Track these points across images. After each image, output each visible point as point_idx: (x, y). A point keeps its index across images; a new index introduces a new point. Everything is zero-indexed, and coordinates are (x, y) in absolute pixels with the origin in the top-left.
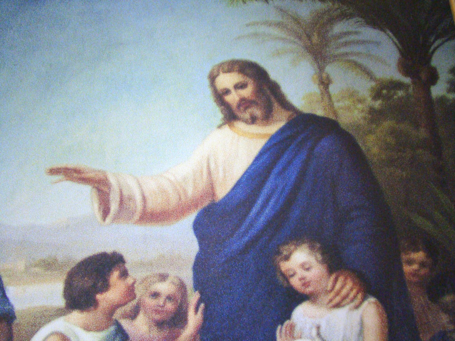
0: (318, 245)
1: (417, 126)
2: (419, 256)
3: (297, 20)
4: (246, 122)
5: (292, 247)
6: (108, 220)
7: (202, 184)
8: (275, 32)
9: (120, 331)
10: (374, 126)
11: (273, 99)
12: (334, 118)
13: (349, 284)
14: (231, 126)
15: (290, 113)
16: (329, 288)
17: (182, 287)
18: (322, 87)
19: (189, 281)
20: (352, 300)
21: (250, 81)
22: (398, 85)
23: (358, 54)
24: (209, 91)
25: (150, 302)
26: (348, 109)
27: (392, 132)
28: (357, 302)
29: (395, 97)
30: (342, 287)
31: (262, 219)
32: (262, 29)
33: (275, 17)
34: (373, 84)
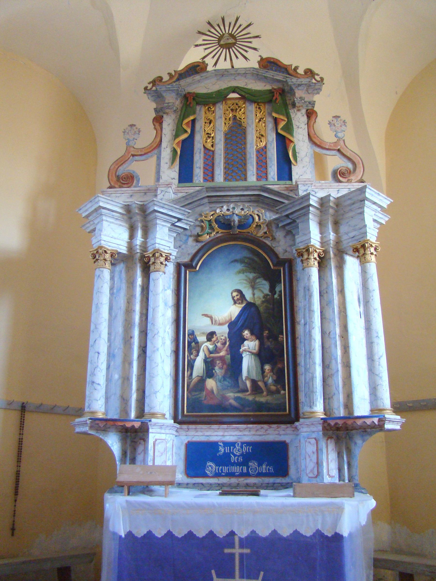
1: (270, 305)
2: (267, 332)
7: (230, 317)
8: (245, 282)
9: (216, 346)
14: (235, 305)
17: (226, 338)
19: (227, 337)
23: (261, 287)
24: (231, 297)
27: (266, 306)
32: (242, 281)
33: (246, 278)
34: (263, 295)
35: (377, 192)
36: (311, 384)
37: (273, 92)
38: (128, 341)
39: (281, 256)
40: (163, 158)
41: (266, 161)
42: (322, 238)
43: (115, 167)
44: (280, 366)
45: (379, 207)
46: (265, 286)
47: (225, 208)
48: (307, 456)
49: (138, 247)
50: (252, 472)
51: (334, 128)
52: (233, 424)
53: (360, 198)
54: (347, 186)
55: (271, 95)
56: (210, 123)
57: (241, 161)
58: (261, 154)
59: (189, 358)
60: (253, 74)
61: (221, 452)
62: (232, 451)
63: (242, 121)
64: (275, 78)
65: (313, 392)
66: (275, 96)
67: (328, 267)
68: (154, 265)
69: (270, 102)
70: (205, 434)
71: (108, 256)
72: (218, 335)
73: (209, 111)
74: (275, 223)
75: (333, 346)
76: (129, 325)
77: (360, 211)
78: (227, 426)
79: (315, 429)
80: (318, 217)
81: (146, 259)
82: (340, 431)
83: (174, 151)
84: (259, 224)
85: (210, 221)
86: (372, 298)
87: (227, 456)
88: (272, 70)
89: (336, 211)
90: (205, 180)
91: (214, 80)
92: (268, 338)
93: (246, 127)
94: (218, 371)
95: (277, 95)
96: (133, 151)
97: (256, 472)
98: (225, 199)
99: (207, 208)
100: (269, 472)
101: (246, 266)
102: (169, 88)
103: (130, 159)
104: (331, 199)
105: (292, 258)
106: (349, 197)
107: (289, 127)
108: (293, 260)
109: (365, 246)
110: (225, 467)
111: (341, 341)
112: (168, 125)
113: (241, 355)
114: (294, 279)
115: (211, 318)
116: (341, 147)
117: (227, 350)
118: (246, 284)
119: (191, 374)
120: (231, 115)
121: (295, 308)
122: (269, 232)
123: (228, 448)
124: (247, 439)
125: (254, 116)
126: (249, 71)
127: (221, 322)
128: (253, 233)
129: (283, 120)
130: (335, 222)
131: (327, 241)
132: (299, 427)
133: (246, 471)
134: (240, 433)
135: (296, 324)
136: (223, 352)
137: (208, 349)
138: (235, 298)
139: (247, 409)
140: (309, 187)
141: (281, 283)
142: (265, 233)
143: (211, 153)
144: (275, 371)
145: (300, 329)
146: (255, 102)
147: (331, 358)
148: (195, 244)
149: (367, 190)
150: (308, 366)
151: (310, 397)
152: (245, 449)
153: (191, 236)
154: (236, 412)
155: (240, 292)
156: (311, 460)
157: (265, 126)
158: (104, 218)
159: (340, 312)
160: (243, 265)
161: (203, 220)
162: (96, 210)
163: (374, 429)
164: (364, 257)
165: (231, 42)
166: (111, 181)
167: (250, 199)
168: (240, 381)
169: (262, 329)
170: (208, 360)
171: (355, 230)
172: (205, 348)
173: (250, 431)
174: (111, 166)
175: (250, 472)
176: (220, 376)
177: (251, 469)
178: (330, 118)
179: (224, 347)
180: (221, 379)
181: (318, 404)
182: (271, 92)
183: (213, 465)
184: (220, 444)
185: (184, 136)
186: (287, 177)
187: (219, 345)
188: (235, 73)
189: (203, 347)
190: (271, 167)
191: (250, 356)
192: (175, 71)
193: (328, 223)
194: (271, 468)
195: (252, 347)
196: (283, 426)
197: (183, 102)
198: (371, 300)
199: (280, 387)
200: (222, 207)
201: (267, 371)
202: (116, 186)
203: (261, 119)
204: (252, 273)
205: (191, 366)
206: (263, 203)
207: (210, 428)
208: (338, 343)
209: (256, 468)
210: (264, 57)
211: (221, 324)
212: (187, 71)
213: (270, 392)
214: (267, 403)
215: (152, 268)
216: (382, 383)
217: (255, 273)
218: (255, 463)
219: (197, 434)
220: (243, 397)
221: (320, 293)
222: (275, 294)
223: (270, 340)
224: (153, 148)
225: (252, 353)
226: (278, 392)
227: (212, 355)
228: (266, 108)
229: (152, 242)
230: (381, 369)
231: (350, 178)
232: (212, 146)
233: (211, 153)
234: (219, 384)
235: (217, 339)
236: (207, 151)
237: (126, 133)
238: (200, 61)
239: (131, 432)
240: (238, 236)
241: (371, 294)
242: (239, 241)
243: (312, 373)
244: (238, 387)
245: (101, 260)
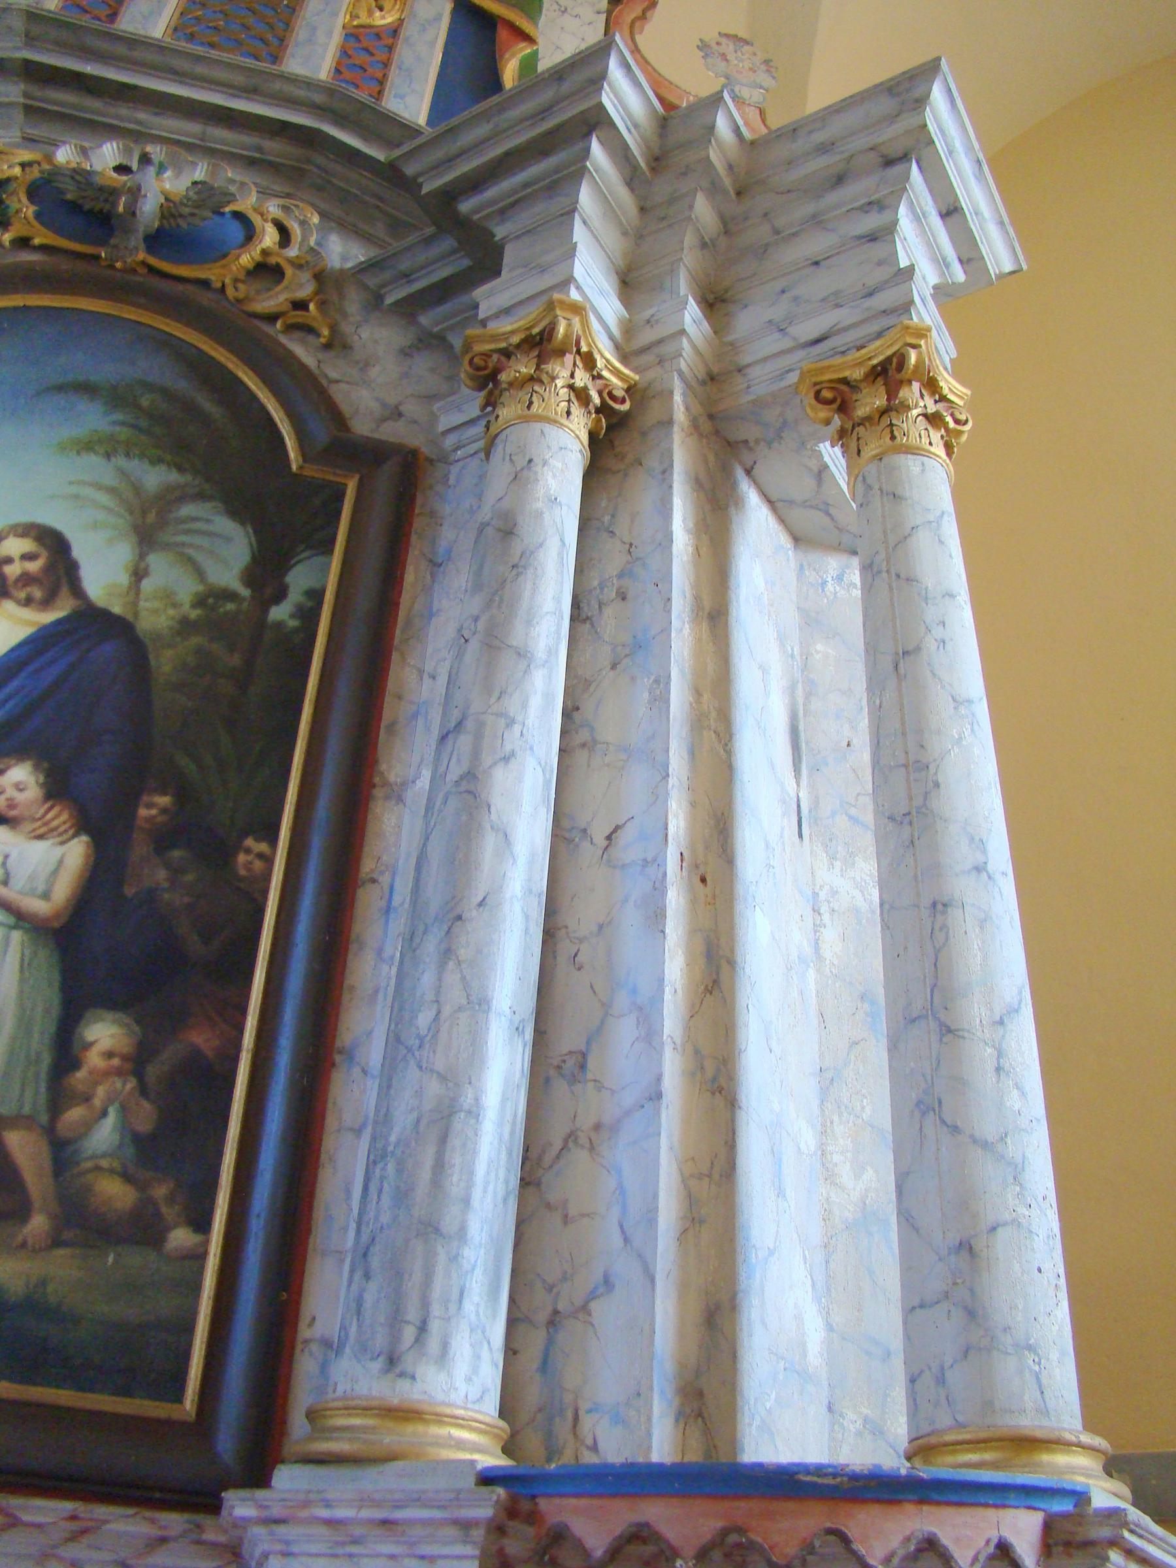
0: (46, 765)
2: (164, 800)
3: (137, 489)
4: (19, 602)
5: (13, 762)
8: (104, 499)
10: (178, 639)
11: (64, 580)
12: (131, 620)
13: (65, 816)
15: (79, 602)
16: (39, 815)
18: (133, 579)
20: (60, 834)
21: (44, 554)
22: (230, 595)
23: (199, 548)
26: (155, 612)
27: (199, 651)
28: (65, 837)
29: (221, 610)
30: (53, 819)
32: (88, 492)
33: (110, 479)
34: (201, 588)
36: (429, 1163)
39: (362, 427)
42: (628, 329)
53: (890, 135)
65: (430, 1229)
67: (653, 461)
74: (366, 288)
75: (631, 921)
77: (871, 222)
80: (625, 234)
84: (273, 260)
86: (938, 632)
89: (728, 226)
92: (163, 840)
98: (123, 114)
99: (15, 135)
101: (134, 426)
104: (722, 124)
105: (425, 450)
106: (820, 137)
108: (431, 461)
111: (693, 901)
114: (413, 555)
118: (110, 510)
121: (388, 699)
122: (323, 304)
128: (230, 292)
130: (711, 298)
131: (660, 342)
132: (259, 1539)
135: (378, 792)
141: (331, 552)
145: (399, 827)
147: (606, 1006)
149: (937, 93)
150: (424, 1019)
151: (397, 1274)
159: (697, 722)
160: (119, 416)
167: (260, 149)
178: (711, 36)
181: (462, 1347)
193: (673, 272)
195: (32, 878)
198: (930, 644)
199: (171, 1199)
201: (94, 1059)
204: (164, 468)
208: (675, 899)
216: (1023, 1210)
217: (181, 469)
221: (576, 604)
222: (280, 595)
223: (177, 854)
230: (1013, 1101)
241: (931, 613)
242: (139, 306)
243: (443, 1078)
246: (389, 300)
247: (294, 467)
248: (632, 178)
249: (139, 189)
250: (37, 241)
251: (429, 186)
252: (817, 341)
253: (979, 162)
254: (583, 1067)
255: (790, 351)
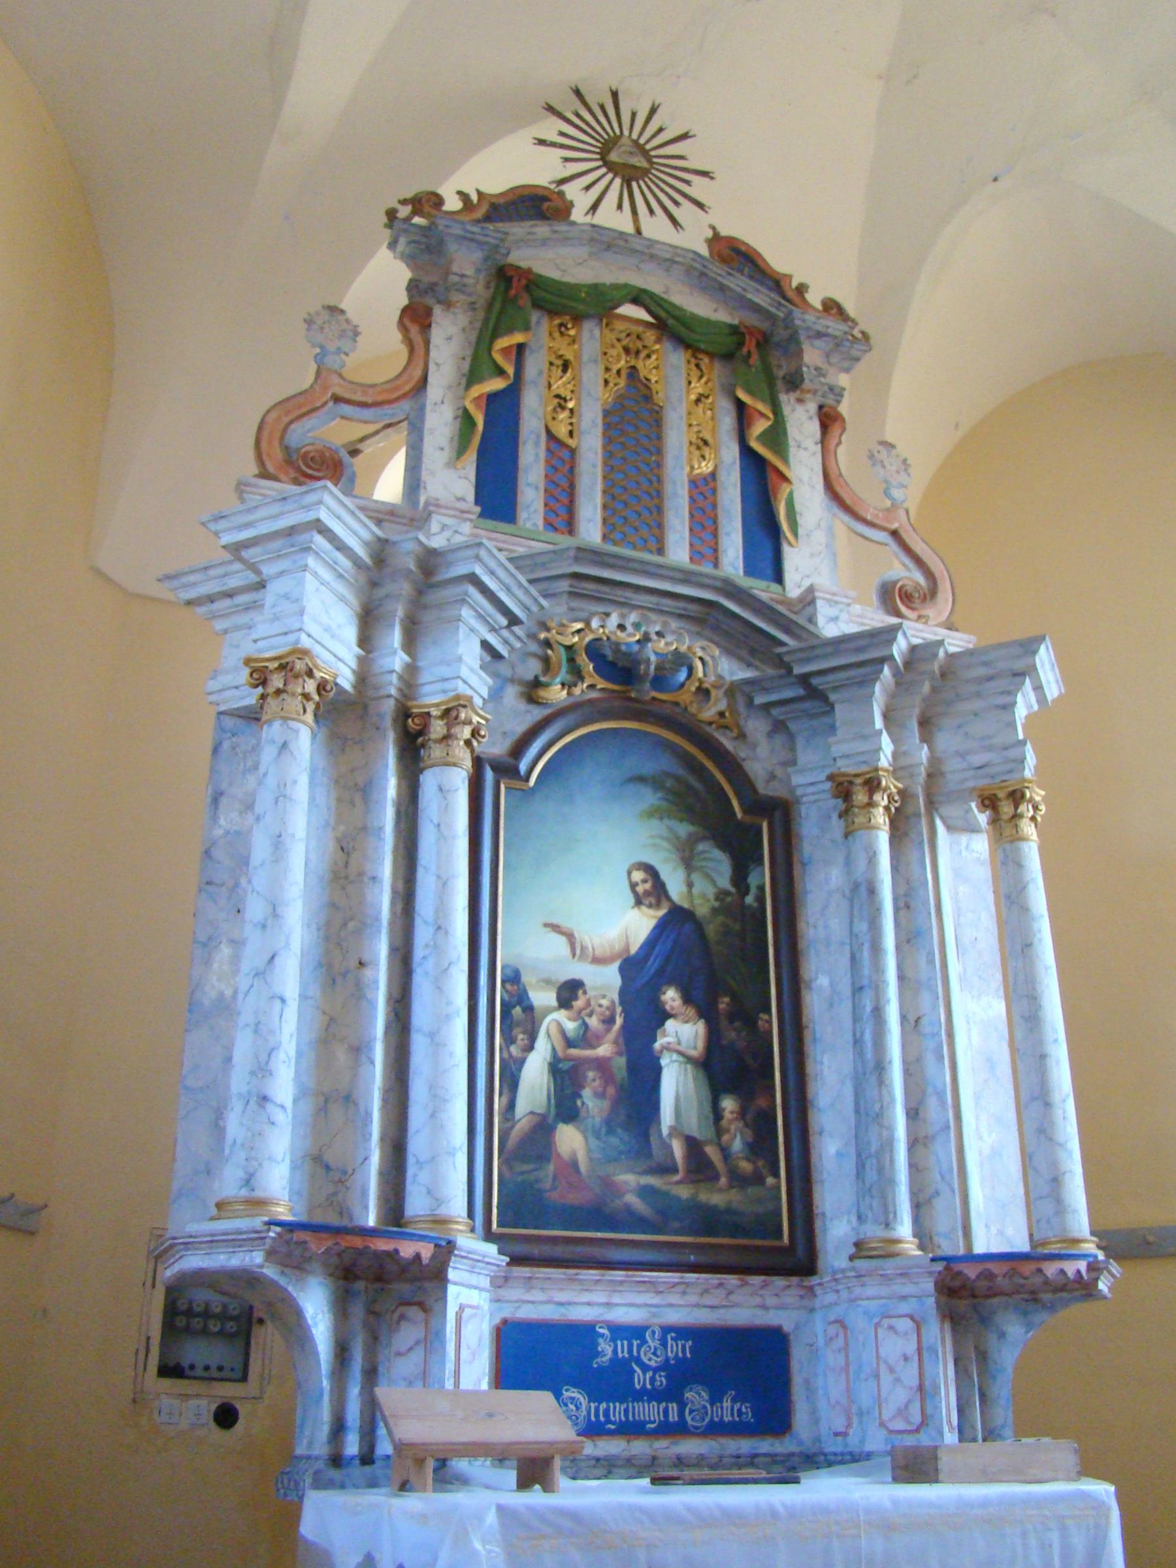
2: (727, 999)
3: (678, 838)
6: (576, 958)
7: (623, 944)
8: (665, 844)
14: (639, 908)
19: (617, 1001)
22: (727, 893)
25: (598, 1009)
26: (701, 905)
31: (653, 970)
32: (658, 841)
33: (665, 833)
35: (1054, 661)
36: (888, 1159)
37: (743, 334)
38: (344, 975)
39: (763, 789)
40: (432, 431)
41: (716, 515)
43: (279, 419)
44: (761, 1102)
45: (1038, 701)
46: (720, 866)
47: (614, 620)
48: (883, 1368)
49: (394, 679)
50: (692, 1419)
51: (882, 471)
52: (643, 1270)
53: (1019, 665)
54: (921, 631)
55: (735, 339)
56: (565, 370)
57: (648, 499)
58: (701, 493)
59: (506, 1055)
60: (689, 270)
61: (605, 1355)
62: (635, 1353)
63: (654, 387)
64: (749, 296)
66: (747, 344)
67: (913, 836)
68: (443, 744)
69: (728, 357)
70: (556, 1299)
71: (311, 686)
72: (591, 993)
73: (562, 334)
74: (743, 693)
76: (351, 925)
77: (1005, 699)
78: (627, 1276)
79: (909, 1289)
81: (416, 720)
82: (960, 1298)
83: (466, 419)
85: (569, 648)
86: (1038, 936)
87: (621, 1368)
88: (741, 272)
89: (934, 690)
90: (549, 525)
91: (582, 252)
92: (732, 1017)
93: (661, 407)
94: (592, 1102)
95: (750, 345)
96: (340, 386)
97: (704, 1420)
98: (620, 594)
100: (740, 1420)
101: (667, 800)
102: (473, 233)
103: (326, 408)
104: (941, 653)
107: (777, 436)
109: (1023, 796)
110: (617, 1404)
112: (447, 339)
113: (659, 1058)
115: (570, 937)
116: (901, 526)
117: (616, 1042)
119: (511, 1106)
120: (623, 362)
121: (799, 940)
123: (625, 1343)
124: (675, 1317)
125: (684, 383)
126: (684, 257)
127: (599, 953)
129: (762, 415)
131: (911, 766)
133: (676, 1419)
134: (656, 1300)
135: (802, 986)
136: (606, 1045)
137: (563, 1033)
138: (640, 889)
139: (676, 1224)
140: (841, 611)
142: (721, 714)
143: (566, 454)
144: (749, 1117)
146: (688, 346)
147: (924, 1092)
148: (522, 706)
149: (1042, 649)
152: (676, 1349)
153: (512, 681)
154: (645, 1233)
155: (651, 871)
156: (898, 1380)
157: (712, 418)
158: (311, 561)
160: (659, 795)
161: (552, 641)
162: (291, 531)
163: (1064, 1294)
164: (1013, 822)
165: (638, 164)
166: (265, 458)
168: (654, 1140)
169: (714, 991)
170: (561, 1065)
171: (990, 749)
172: (554, 1031)
173: (684, 1293)
174: (268, 411)
175: (688, 1418)
176: (598, 1120)
177: (691, 1411)
179: (608, 1030)
180: (601, 1128)
182: (734, 330)
183: (582, 1399)
184: (601, 1331)
185: (496, 384)
186: (769, 572)
187: (594, 1022)
188: (646, 251)
189: (547, 1024)
190: (728, 534)
191: (683, 1066)
192: (479, 193)
194: (746, 1408)
196: (779, 1282)
197: (493, 285)
198: (1036, 941)
200: (608, 615)
201: (727, 1115)
202: (282, 476)
203: (703, 399)
205: (512, 1081)
206: (716, 628)
207: (571, 1280)
209: (704, 1407)
210: (724, 232)
211: (597, 960)
212: (513, 203)
213: (738, 1180)
214: (729, 1211)
215: (436, 752)
218: (703, 1394)
219: (528, 1297)
220: (665, 1188)
222: (747, 892)
223: (737, 1024)
224: (402, 392)
225: (689, 1059)
226: (758, 1179)
227: (574, 1052)
228: (717, 371)
229: (445, 671)
231: (924, 612)
232: (571, 433)
233: (566, 454)
234: (594, 1142)
235: (588, 1004)
236: (553, 446)
237: (315, 327)
238: (552, 187)
239: (367, 1279)
240: (648, 707)
242: (652, 724)
244: (649, 1155)
245: (293, 694)
246: (759, 700)
247: (739, 815)
248: (896, 673)
249: (649, 659)
250: (599, 687)
251: (798, 670)
252: (980, 768)
253: (1053, 665)
254: (917, 1114)
255: (964, 770)
